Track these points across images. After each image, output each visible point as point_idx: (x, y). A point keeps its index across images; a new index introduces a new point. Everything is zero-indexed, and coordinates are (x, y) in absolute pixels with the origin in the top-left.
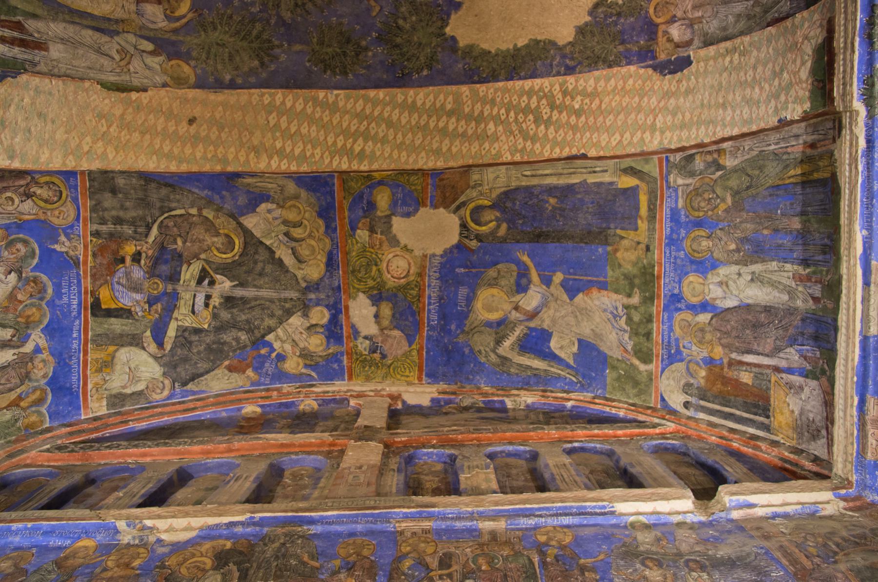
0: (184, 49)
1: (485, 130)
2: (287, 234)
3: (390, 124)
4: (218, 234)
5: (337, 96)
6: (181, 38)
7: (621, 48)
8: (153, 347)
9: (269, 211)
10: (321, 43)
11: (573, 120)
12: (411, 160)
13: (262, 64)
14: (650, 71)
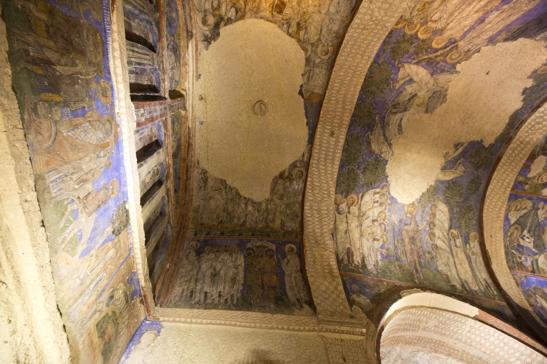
0: (466, 234)
2: (518, 211)
4: (514, 232)
8: (537, 256)
13: (472, 210)
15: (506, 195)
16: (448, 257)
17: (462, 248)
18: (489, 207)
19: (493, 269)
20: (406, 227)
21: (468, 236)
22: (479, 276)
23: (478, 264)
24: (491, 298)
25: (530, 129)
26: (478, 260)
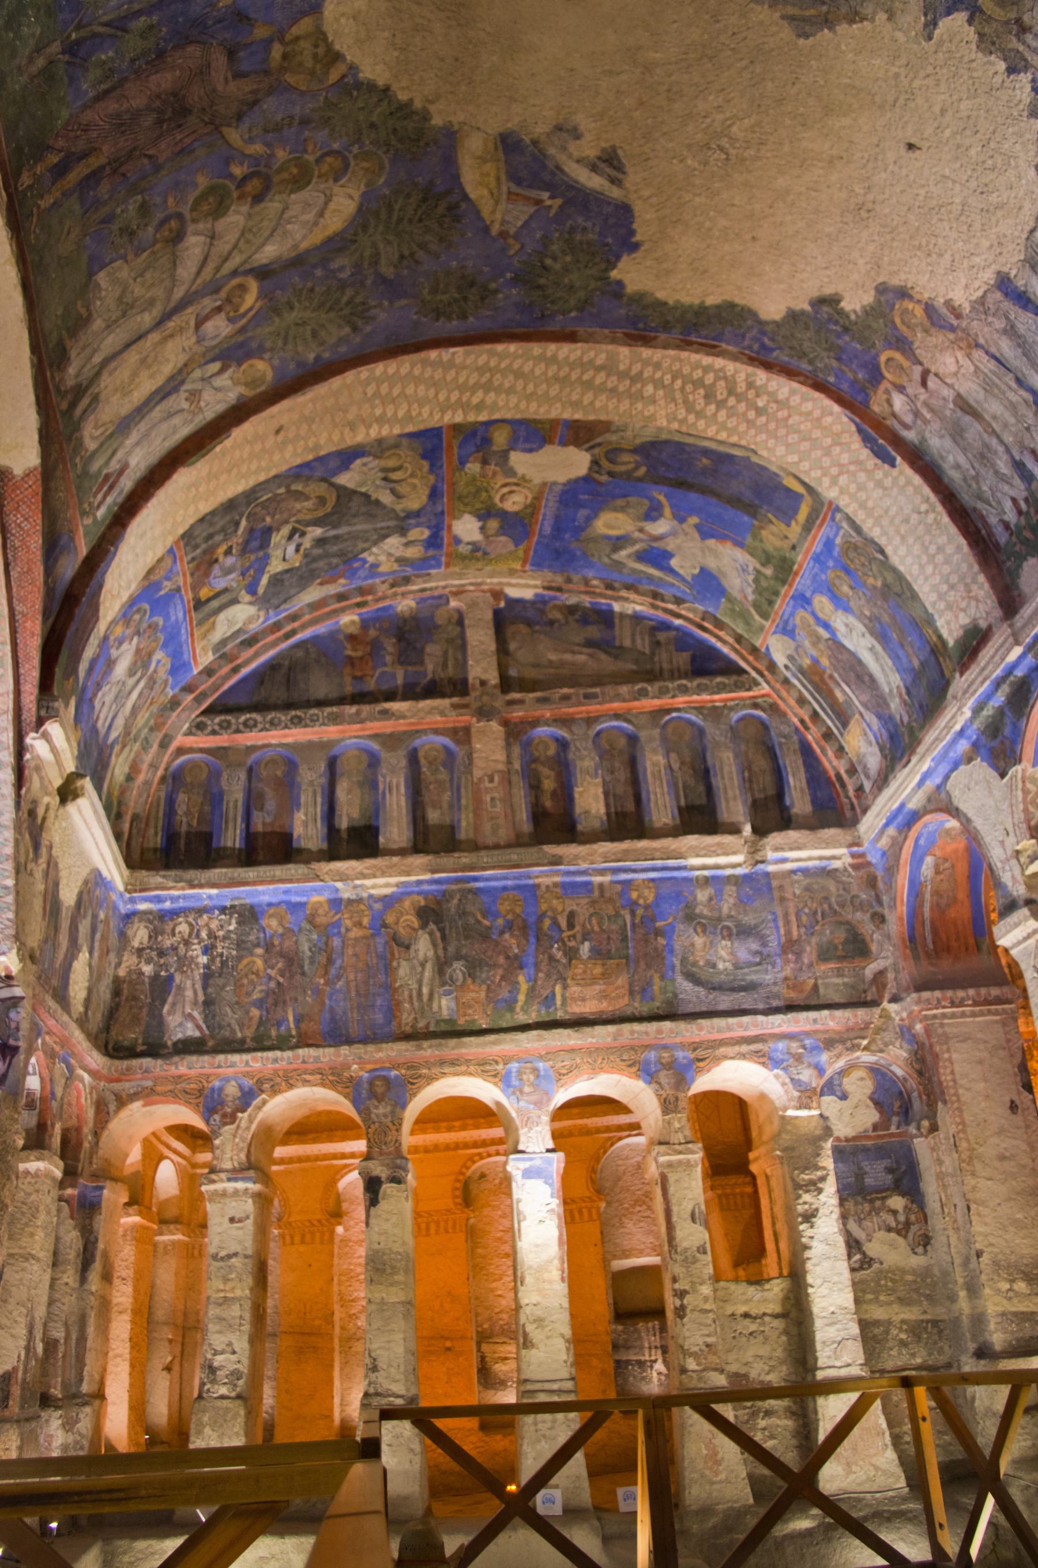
0: (254, 345)
1: (641, 391)
2: (385, 479)
3: (519, 374)
5: (454, 354)
6: (249, 334)
7: (835, 364)
8: (248, 598)
9: (364, 465)
10: (434, 291)
11: (752, 414)
12: (542, 410)
13: (355, 329)
14: (853, 428)
15: (437, 416)
16: (152, 302)
17: (200, 349)
18: (380, 382)
19: (175, 477)
20: (219, 60)
21: (249, 355)
22: (129, 442)
23: (164, 427)
24: (81, 503)
25: (687, 380)
26: (177, 420)
